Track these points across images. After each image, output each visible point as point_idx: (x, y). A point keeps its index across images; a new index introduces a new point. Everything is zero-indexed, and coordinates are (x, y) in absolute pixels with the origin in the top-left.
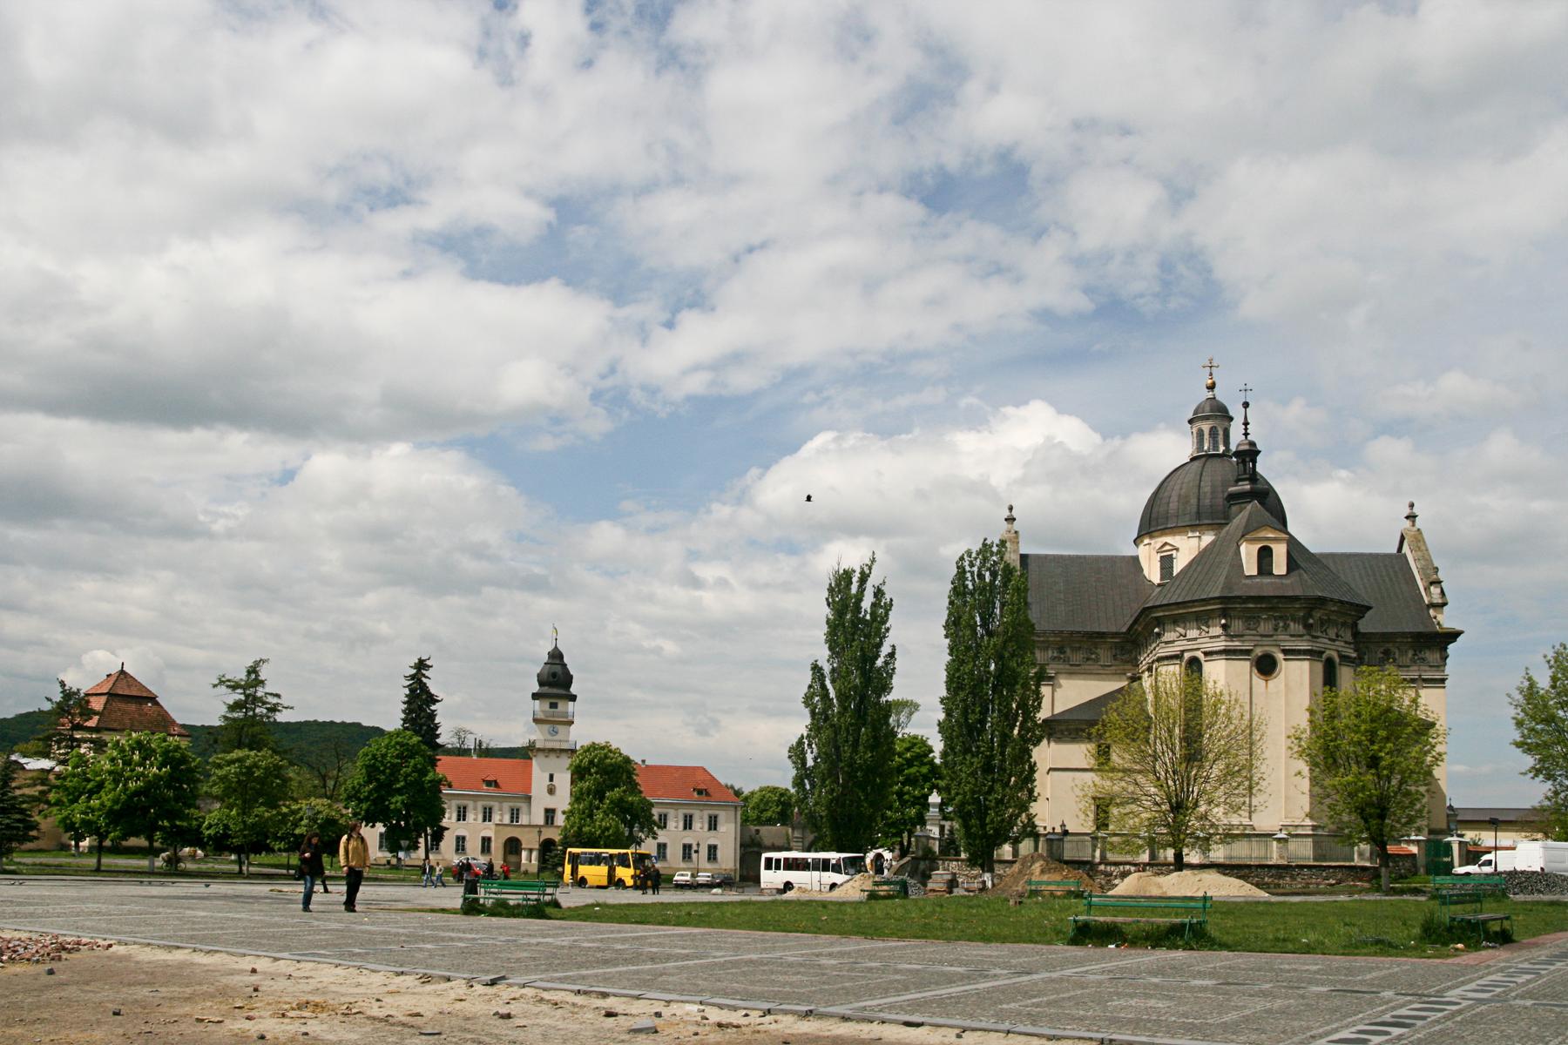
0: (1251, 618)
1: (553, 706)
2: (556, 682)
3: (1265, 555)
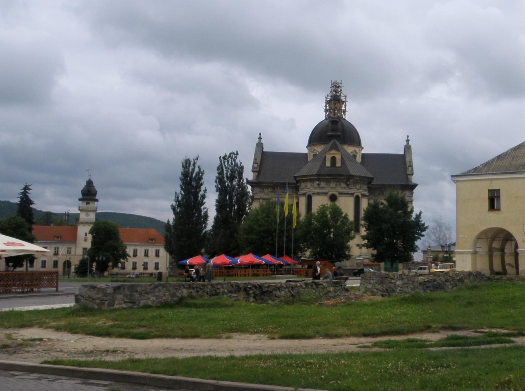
0: (328, 181)
1: (87, 203)
2: (89, 194)
3: (333, 159)
